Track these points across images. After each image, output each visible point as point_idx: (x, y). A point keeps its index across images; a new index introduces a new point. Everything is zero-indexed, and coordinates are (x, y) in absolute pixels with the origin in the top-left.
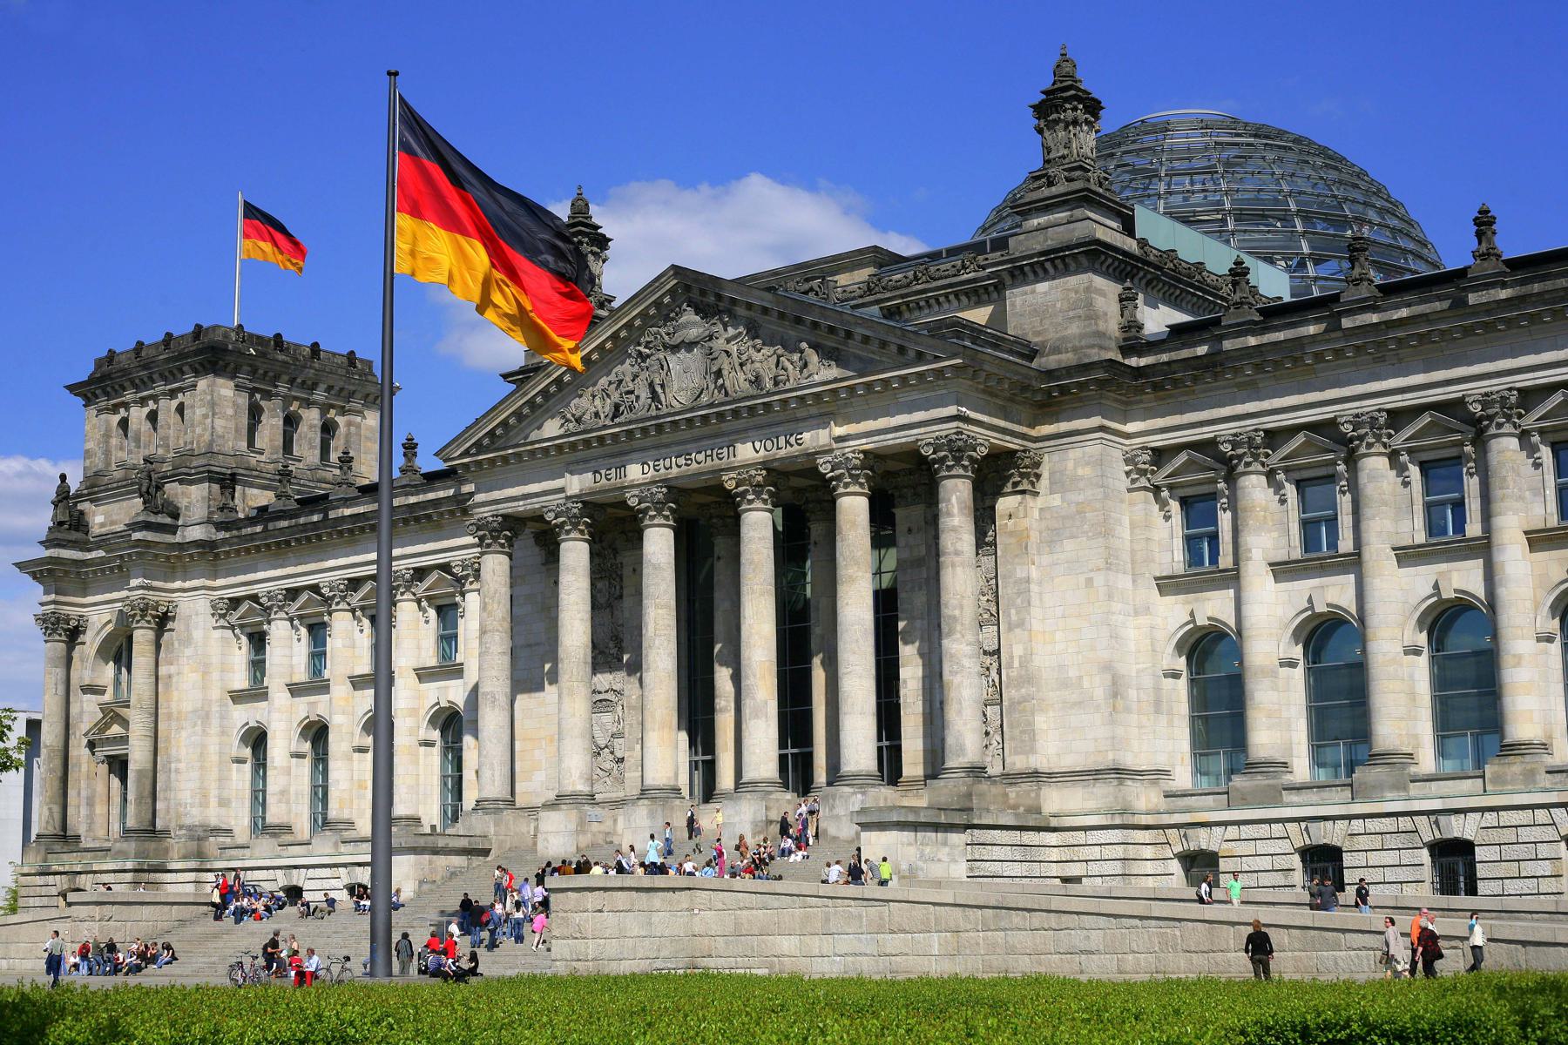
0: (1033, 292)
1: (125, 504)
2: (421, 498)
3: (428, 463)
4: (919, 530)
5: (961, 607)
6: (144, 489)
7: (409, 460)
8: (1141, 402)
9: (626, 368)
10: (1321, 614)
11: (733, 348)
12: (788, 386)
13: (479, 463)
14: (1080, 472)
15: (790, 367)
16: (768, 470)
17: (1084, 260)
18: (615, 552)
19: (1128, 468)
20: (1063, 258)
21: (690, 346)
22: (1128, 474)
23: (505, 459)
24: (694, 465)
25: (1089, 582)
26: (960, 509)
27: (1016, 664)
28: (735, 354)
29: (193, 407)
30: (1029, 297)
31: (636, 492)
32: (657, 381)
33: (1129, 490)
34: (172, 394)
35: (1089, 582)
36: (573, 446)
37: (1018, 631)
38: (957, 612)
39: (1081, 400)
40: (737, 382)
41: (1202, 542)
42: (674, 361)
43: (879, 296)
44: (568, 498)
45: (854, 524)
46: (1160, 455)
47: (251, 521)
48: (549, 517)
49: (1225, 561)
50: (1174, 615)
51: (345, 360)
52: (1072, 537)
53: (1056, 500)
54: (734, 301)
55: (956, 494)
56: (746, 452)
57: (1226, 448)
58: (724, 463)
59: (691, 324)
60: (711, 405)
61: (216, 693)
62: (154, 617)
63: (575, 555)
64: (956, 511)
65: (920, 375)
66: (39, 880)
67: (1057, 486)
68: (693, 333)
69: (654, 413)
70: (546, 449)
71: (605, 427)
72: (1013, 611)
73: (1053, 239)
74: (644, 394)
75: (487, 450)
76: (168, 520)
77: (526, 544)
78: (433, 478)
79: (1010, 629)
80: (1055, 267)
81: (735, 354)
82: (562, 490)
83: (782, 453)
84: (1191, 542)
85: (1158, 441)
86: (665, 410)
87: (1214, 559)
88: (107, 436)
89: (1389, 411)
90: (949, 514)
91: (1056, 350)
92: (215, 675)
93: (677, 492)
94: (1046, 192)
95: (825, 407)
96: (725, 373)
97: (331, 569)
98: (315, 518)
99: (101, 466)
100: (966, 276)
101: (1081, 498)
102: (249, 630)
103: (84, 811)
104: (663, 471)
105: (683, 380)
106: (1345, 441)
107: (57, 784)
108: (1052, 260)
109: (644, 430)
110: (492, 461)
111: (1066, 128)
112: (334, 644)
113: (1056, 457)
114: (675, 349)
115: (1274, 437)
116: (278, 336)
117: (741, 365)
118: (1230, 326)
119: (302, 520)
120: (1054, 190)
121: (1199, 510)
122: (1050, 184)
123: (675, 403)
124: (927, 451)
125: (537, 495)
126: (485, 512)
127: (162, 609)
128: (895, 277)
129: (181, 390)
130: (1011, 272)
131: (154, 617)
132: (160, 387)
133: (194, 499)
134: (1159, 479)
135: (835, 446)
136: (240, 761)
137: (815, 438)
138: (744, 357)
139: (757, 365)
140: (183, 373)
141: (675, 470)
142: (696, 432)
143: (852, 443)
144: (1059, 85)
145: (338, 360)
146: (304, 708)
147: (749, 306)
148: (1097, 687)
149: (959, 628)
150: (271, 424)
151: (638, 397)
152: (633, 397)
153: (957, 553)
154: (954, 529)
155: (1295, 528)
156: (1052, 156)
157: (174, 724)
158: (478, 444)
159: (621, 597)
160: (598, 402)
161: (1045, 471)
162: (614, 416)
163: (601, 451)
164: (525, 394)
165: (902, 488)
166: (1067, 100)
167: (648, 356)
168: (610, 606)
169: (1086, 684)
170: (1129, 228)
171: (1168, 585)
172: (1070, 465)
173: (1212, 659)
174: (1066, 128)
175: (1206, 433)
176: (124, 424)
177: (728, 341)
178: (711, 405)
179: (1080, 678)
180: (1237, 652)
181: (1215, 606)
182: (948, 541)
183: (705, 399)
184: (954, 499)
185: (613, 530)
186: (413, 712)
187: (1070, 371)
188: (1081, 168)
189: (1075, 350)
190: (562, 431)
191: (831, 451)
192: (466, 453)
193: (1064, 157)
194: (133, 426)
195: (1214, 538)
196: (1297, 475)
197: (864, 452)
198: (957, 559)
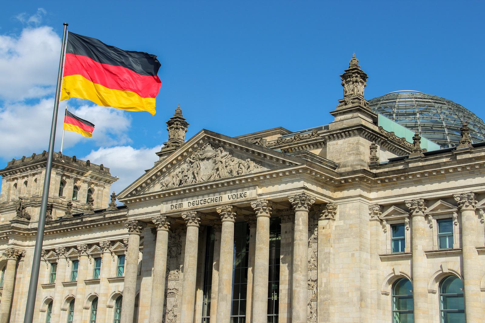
0: (337, 144)
1: (12, 214)
2: (116, 215)
3: (118, 203)
4: (289, 232)
5: (301, 261)
6: (18, 208)
7: (113, 201)
8: (376, 187)
9: (185, 166)
10: (446, 273)
11: (223, 160)
12: (242, 174)
13: (131, 200)
14: (351, 212)
15: (243, 168)
16: (233, 206)
17: (356, 131)
18: (180, 236)
19: (370, 212)
20: (348, 131)
21: (208, 159)
22: (370, 214)
24: (207, 204)
25: (353, 255)
26: (303, 223)
27: (323, 286)
28: (224, 163)
29: (40, 180)
30: (335, 146)
31: (185, 213)
32: (195, 172)
33: (370, 220)
34: (34, 175)
35: (353, 255)
36: (164, 195)
37: (324, 273)
38: (299, 263)
39: (353, 185)
40: (224, 173)
41: (398, 241)
42: (202, 163)
43: (280, 145)
44: (161, 214)
45: (263, 228)
46: (383, 208)
47: (56, 222)
48: (154, 221)
49: (407, 250)
50: (388, 270)
51: (99, 167)
52: (347, 237)
53: (341, 223)
54: (225, 143)
55: (302, 217)
56: (226, 198)
57: (408, 205)
58: (217, 203)
59: (209, 151)
60: (214, 181)
62: (16, 255)
63: (163, 235)
64: (301, 224)
65: (290, 172)
67: (342, 217)
68: (209, 154)
69: (193, 183)
70: (154, 196)
71: (176, 188)
72: (323, 265)
73: (345, 124)
74: (191, 176)
75: (135, 195)
76: (26, 220)
77: (147, 231)
78: (120, 208)
79: (321, 272)
80: (345, 135)
81: (224, 163)
82: (159, 211)
83: (239, 200)
84: (395, 241)
85: (382, 202)
86: (197, 182)
87: (403, 249)
88: (9, 190)
89: (475, 193)
90: (298, 225)
91: (345, 166)
93: (200, 214)
94: (344, 107)
95: (254, 182)
96: (220, 169)
97: (80, 239)
98: (78, 221)
99: (6, 200)
100: (313, 139)
101: (351, 222)
102: (52, 262)
104: (196, 205)
105: (205, 171)
106: (456, 204)
108: (344, 132)
109: (190, 190)
110: (135, 200)
111: (353, 83)
112: (81, 267)
113: (342, 206)
114: (203, 160)
115: (428, 202)
116: (75, 157)
117: (226, 167)
118: (412, 159)
119: (74, 222)
120: (347, 107)
121: (397, 229)
122: (346, 104)
123: (201, 180)
124: (291, 200)
125: (150, 213)
126: (131, 219)
127: (20, 253)
128: (287, 139)
129: (36, 174)
130: (329, 136)
131: (16, 255)
132: (30, 172)
133: (35, 213)
134: (382, 216)
135: (258, 197)
137: (250, 193)
138: (227, 164)
139: (232, 167)
140: (38, 168)
141: (200, 206)
142: (208, 191)
143: (264, 197)
144: (351, 68)
145: (97, 167)
146: (68, 292)
147: (230, 145)
148: (355, 296)
149: (300, 269)
150: (68, 190)
151: (188, 178)
152: (187, 178)
153: (301, 240)
154: (300, 231)
155: (436, 238)
156: (347, 94)
157: (20, 296)
158: (131, 193)
159: (181, 253)
160: (174, 179)
161: (338, 211)
162: (180, 184)
163: (174, 197)
164: (148, 175)
165: (282, 215)
166: (353, 73)
167: (193, 163)
168: (177, 257)
169: (350, 295)
170: (375, 123)
171: (384, 258)
172: (348, 209)
173: (401, 286)
174: (353, 83)
175: (401, 199)
176: (16, 185)
177: (222, 158)
178: (214, 181)
179: (348, 293)
180: (411, 287)
181: (402, 267)
182: (297, 235)
183: (212, 179)
184: (300, 219)
185: (177, 227)
187: (348, 173)
188: (357, 98)
189: (352, 166)
190: (161, 190)
191: (256, 199)
192: (127, 197)
193: (351, 95)
194: (18, 186)
195: (403, 240)
196: (438, 218)
197: (269, 200)
198: (301, 242)
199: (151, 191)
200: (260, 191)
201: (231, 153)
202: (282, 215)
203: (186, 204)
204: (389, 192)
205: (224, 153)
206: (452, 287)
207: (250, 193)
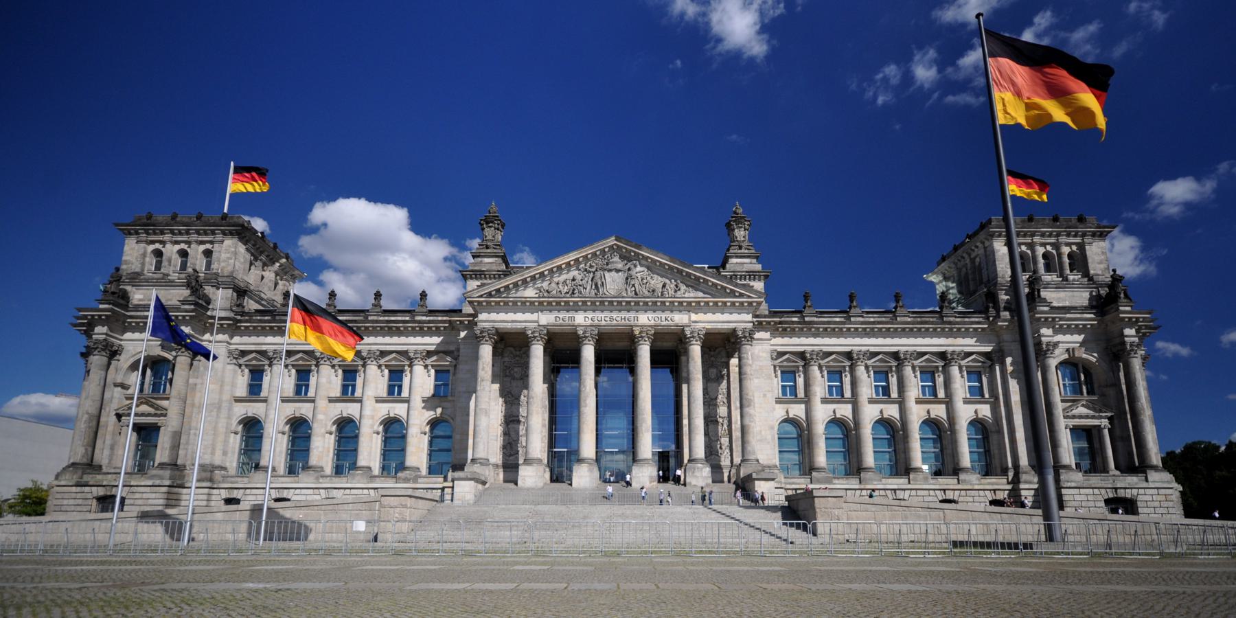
21: (618, 271)
23: (506, 303)
35: (765, 396)
42: (607, 274)
50: (780, 412)
56: (645, 319)
59: (617, 262)
61: (226, 396)
65: (742, 303)
66: (79, 489)
68: (620, 266)
85: (780, 349)
88: (144, 255)
92: (227, 388)
95: (689, 307)
103: (107, 452)
107: (92, 435)
114: (610, 271)
121: (788, 374)
132: (194, 237)
134: (777, 362)
136: (236, 433)
141: (603, 323)
157: (195, 410)
171: (779, 401)
181: (798, 411)
186: (372, 417)
199: (519, 294)
200: (694, 317)
201: (649, 268)
202: (723, 347)
203: (580, 319)
204: (786, 340)
205: (639, 268)
206: (348, 432)
207: (680, 318)
